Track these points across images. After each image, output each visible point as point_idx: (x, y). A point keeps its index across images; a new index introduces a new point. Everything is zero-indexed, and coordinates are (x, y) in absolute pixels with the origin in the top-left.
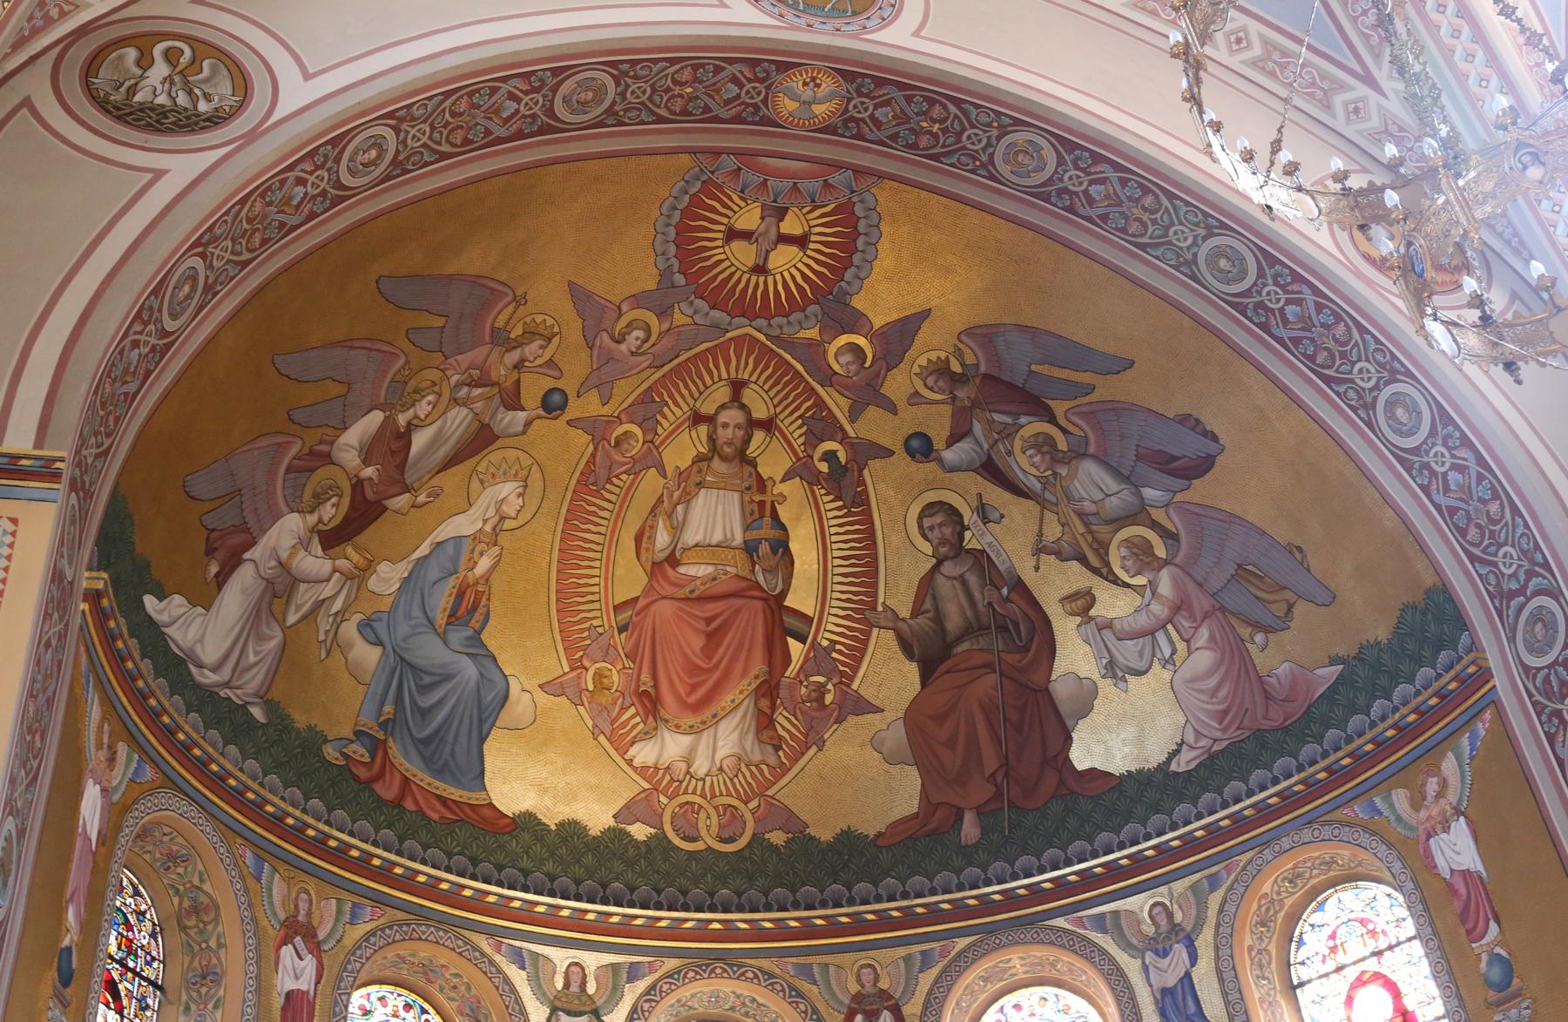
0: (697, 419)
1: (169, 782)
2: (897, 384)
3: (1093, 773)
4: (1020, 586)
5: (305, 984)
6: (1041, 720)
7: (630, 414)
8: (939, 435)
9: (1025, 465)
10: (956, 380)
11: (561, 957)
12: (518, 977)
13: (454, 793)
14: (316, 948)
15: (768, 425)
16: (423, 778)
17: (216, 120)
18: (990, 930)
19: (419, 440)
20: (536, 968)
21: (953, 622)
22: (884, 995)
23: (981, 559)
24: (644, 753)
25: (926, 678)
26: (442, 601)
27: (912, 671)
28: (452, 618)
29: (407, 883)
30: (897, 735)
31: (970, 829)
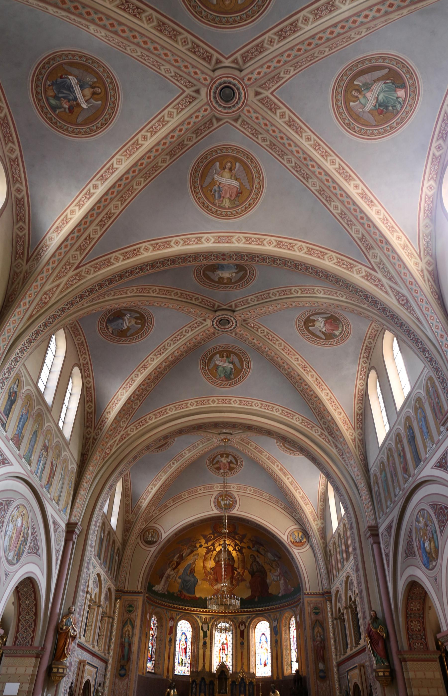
0: (220, 545)
1: (157, 607)
2: (245, 541)
3: (271, 594)
4: (262, 566)
5: (172, 625)
6: (265, 586)
7: (211, 545)
8: (251, 546)
10: (252, 541)
11: (204, 616)
12: (198, 620)
13: (191, 596)
14: (173, 620)
15: (230, 545)
16: (187, 595)
17: (156, 542)
18: (257, 614)
19: (184, 555)
21: (255, 570)
22: (244, 622)
23: (257, 562)
24: (216, 587)
25: (252, 577)
26: (189, 571)
27: (250, 576)
28: (190, 573)
29: (185, 609)
30: (248, 584)
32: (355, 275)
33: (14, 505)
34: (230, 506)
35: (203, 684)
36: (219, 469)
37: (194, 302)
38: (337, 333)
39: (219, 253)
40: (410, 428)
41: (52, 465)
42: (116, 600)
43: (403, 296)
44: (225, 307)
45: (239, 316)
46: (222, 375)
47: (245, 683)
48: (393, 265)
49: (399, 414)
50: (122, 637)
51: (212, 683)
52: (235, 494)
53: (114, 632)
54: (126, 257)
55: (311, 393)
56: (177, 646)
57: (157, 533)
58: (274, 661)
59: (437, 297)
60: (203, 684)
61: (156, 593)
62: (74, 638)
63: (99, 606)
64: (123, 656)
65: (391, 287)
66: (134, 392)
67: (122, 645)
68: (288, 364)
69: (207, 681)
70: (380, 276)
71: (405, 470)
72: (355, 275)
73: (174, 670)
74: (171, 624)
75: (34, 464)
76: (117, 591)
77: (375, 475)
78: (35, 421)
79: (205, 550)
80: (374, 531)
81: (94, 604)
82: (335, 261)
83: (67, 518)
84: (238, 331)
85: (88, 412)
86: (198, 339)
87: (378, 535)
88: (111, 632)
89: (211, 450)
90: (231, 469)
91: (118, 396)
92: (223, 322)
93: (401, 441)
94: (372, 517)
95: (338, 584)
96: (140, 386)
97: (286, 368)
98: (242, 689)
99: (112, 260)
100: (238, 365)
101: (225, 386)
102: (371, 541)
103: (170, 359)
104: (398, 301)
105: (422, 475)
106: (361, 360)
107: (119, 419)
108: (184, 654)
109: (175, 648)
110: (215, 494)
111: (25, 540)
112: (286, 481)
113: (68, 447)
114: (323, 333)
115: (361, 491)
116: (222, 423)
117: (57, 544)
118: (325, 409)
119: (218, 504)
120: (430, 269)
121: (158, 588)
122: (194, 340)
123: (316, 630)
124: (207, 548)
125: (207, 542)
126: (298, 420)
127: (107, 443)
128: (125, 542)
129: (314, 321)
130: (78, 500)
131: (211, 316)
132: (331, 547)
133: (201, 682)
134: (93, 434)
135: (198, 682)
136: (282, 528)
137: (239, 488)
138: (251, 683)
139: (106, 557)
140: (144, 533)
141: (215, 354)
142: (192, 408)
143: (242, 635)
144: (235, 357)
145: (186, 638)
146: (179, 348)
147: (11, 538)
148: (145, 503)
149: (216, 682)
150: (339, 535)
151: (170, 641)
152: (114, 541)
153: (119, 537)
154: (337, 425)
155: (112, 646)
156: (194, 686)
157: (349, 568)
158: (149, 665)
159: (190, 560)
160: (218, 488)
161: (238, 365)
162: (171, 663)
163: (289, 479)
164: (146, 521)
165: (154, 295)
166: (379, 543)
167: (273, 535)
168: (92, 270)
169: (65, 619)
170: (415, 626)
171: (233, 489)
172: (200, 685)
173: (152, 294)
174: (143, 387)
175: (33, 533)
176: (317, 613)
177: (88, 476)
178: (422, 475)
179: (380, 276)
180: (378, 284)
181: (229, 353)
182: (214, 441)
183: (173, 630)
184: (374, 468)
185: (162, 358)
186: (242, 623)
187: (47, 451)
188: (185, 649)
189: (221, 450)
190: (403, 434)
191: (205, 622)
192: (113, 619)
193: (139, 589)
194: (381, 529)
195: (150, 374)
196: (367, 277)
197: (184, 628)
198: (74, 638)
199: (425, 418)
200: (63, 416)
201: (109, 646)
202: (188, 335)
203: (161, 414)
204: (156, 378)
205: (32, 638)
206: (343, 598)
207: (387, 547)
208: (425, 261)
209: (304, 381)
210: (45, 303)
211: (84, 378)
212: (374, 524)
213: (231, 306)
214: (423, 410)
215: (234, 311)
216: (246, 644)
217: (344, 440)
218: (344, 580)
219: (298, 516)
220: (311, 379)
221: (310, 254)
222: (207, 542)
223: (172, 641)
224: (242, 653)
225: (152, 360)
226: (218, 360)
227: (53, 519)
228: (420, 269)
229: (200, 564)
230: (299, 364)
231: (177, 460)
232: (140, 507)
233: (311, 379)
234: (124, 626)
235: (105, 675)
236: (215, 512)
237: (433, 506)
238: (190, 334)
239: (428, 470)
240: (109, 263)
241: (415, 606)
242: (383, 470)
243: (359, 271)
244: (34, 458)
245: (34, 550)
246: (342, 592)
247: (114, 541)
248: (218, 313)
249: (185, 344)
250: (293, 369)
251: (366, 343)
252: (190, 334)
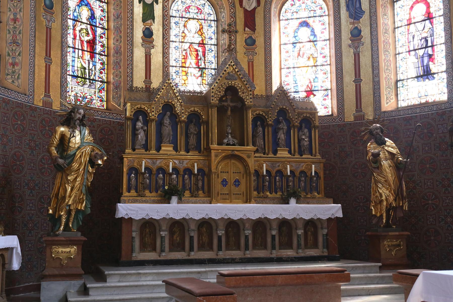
35: (167, 121)
47: (288, 121)
51: (194, 118)
60: (167, 121)
98: (282, 136)
108: (87, 56)
133: (162, 116)
135: (153, 115)
143: (250, 19)
145: (92, 17)
156: (139, 124)
172: (160, 124)
188: (92, 43)
216: (260, 41)
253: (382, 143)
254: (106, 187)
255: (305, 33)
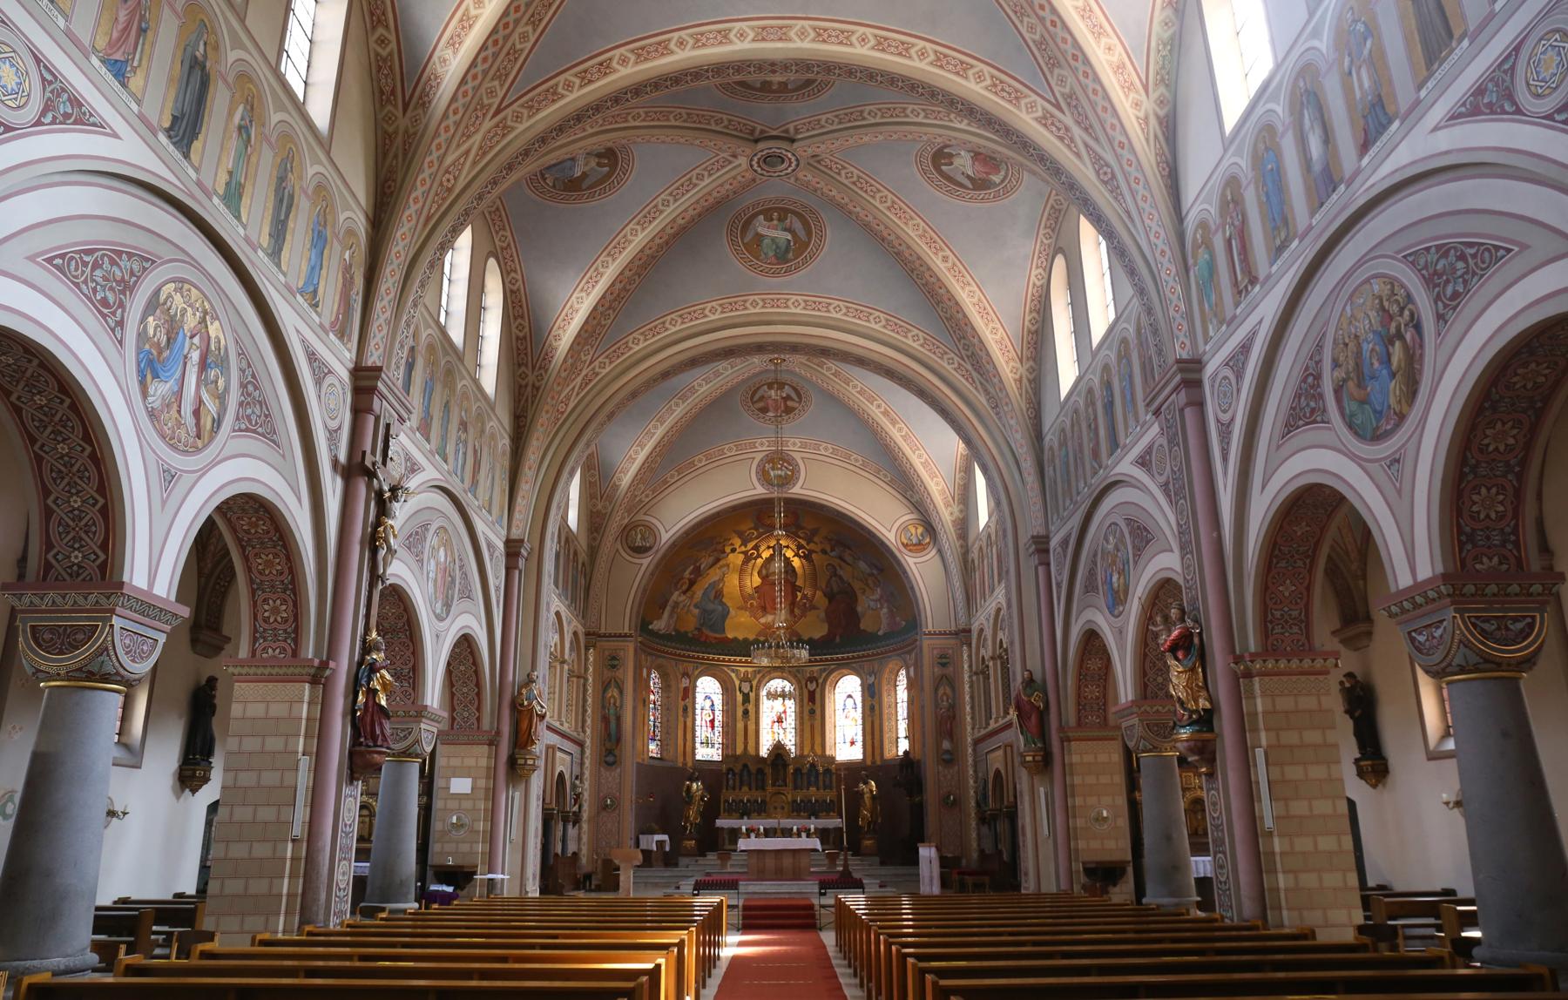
6: (852, 617)
9: (849, 559)
20: (736, 672)
24: (763, 620)
30: (823, 615)
31: (838, 639)
32: (1024, 115)
33: (433, 528)
34: (787, 481)
36: (764, 410)
37: (713, 127)
38: (996, 179)
39: (765, 61)
40: (1108, 385)
41: (475, 451)
42: (587, 649)
43: (1107, 165)
44: (774, 133)
45: (803, 149)
46: (771, 254)
48: (1093, 105)
49: (1094, 354)
50: (603, 707)
51: (760, 771)
52: (797, 456)
53: (590, 700)
54: (586, 80)
55: (942, 291)
56: (698, 718)
57: (651, 531)
58: (869, 738)
59: (1166, 173)
61: (655, 634)
62: (542, 717)
63: (563, 662)
64: (609, 735)
65: (1086, 145)
66: (603, 297)
67: (605, 719)
68: (898, 237)
69: (753, 768)
70: (1068, 120)
71: (1096, 454)
72: (1024, 115)
73: (694, 754)
74: (685, 682)
75: (451, 459)
76: (587, 634)
77: (1051, 448)
78: (445, 385)
79: (742, 557)
80: (1041, 545)
81: (557, 659)
82: (989, 82)
83: (504, 532)
84: (800, 175)
85: (518, 338)
86: (723, 191)
87: (1047, 551)
88: (585, 701)
89: (749, 378)
90: (789, 410)
91: (573, 307)
92: (771, 160)
93: (1093, 404)
94: (1041, 521)
95: (982, 619)
96: (613, 284)
97: (896, 243)
99: (560, 90)
100: (802, 234)
101: (776, 274)
102: (1035, 560)
103: (669, 231)
104: (1097, 173)
105: (1118, 470)
106: (1042, 231)
107: (577, 348)
109: (694, 720)
110: (759, 457)
111: (453, 581)
112: (896, 434)
113: (493, 409)
114: (968, 177)
115: (1025, 475)
116: (772, 344)
117: (496, 579)
118: (968, 323)
119: (764, 476)
120: (1162, 113)
121: (659, 625)
122: (715, 194)
123: (941, 691)
124: (745, 553)
125: (744, 543)
126: (916, 338)
127: (559, 393)
128: (593, 551)
129: (951, 156)
130: (519, 500)
131: (748, 151)
132: (974, 554)
134: (531, 378)
136: (884, 517)
137: (804, 445)
138: (827, 771)
139: (565, 582)
140: (627, 532)
141: (755, 216)
142: (713, 317)
144: (795, 219)
146: (686, 210)
147: (435, 581)
148: (626, 480)
149: (768, 771)
150: (989, 536)
151: (685, 709)
152: (576, 553)
153: (583, 543)
154: (988, 354)
155: (589, 721)
157: (999, 596)
158: (652, 747)
159: (714, 575)
160: (763, 447)
161: (802, 234)
162: (689, 743)
163: (900, 430)
164: (629, 511)
165: (637, 124)
166: (1048, 564)
167: (870, 532)
168: (525, 112)
169: (524, 691)
170: (1092, 691)
171: (793, 446)
173: (632, 123)
174: (618, 286)
175: (461, 567)
176: (943, 665)
177: (532, 456)
178: (1118, 470)
179: (1068, 120)
180: (1065, 136)
181: (784, 213)
182: (757, 362)
183: (689, 693)
184: (1050, 438)
185: (653, 228)
186: (812, 679)
187: (466, 430)
188: (712, 722)
189: (771, 378)
190: (1097, 393)
191: (745, 679)
192: (586, 680)
193: (626, 630)
194: (1054, 542)
195: (631, 262)
196: (1045, 120)
197: (708, 689)
198: (542, 717)
199: (1131, 376)
200: (444, 303)
201: (584, 721)
202: (703, 184)
203: (654, 331)
204: (644, 267)
205: (478, 719)
206: (990, 642)
207: (1060, 574)
208: (1154, 95)
209: (929, 269)
210: (449, 190)
211: (505, 273)
212: (1042, 532)
213: (787, 131)
214: (1130, 364)
215: (793, 141)
216: (818, 712)
217: (1001, 381)
218: (993, 613)
219: (916, 497)
220: (942, 265)
221: (941, 67)
222: (744, 543)
223: (689, 710)
224: (812, 727)
225: (634, 233)
226: (761, 227)
227: (487, 539)
228: (1141, 115)
229: (732, 581)
230: (920, 237)
231: (684, 398)
232: (616, 487)
233: (942, 265)
234: (604, 691)
235: (582, 764)
236: (760, 491)
237: (1129, 521)
238: (707, 181)
239: (1126, 466)
240: (554, 95)
241: (1094, 664)
242: (1063, 444)
243: (1031, 107)
244: (450, 449)
245: (467, 595)
246: (988, 633)
247: (576, 553)
248: (761, 146)
249: (697, 202)
250: (909, 247)
251: (1051, 201)
252: (707, 181)
253: (866, 783)
254: (711, 811)
255: (850, 702)
